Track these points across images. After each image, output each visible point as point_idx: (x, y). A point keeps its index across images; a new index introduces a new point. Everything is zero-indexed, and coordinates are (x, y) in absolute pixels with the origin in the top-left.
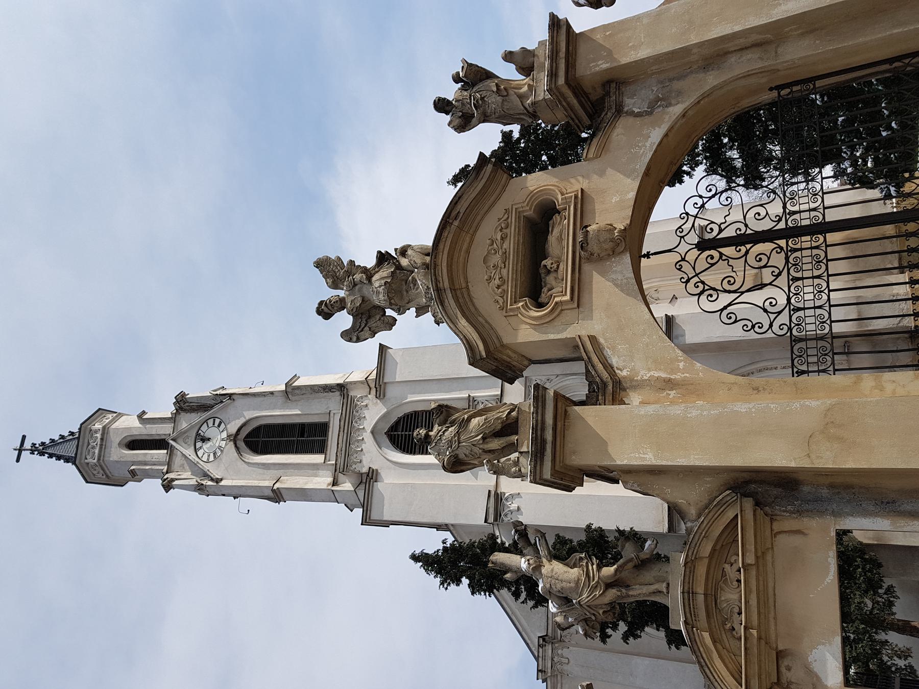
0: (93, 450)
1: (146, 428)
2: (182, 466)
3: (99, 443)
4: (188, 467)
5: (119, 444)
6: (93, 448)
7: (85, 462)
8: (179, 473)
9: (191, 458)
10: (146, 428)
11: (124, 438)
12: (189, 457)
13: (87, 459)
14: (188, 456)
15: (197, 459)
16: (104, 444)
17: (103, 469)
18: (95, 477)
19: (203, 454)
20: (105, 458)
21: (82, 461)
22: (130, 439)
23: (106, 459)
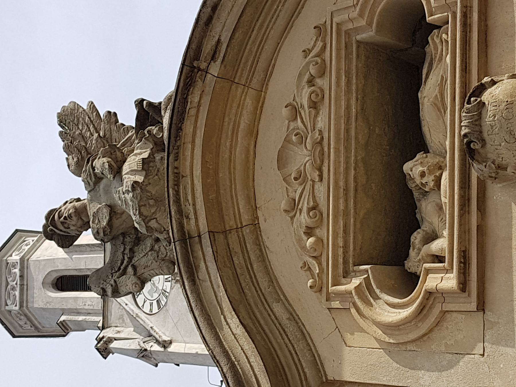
0: (13, 293)
1: (72, 259)
2: (121, 317)
3: (18, 283)
4: (129, 320)
5: (43, 283)
6: (13, 289)
7: (6, 310)
8: (118, 329)
9: (128, 309)
10: (72, 259)
11: (48, 274)
12: (126, 307)
13: (8, 305)
14: (124, 305)
15: (136, 310)
16: (25, 284)
17: (29, 319)
18: (23, 329)
19: (144, 302)
20: (29, 304)
21: (3, 309)
22: (55, 275)
23: (30, 305)
